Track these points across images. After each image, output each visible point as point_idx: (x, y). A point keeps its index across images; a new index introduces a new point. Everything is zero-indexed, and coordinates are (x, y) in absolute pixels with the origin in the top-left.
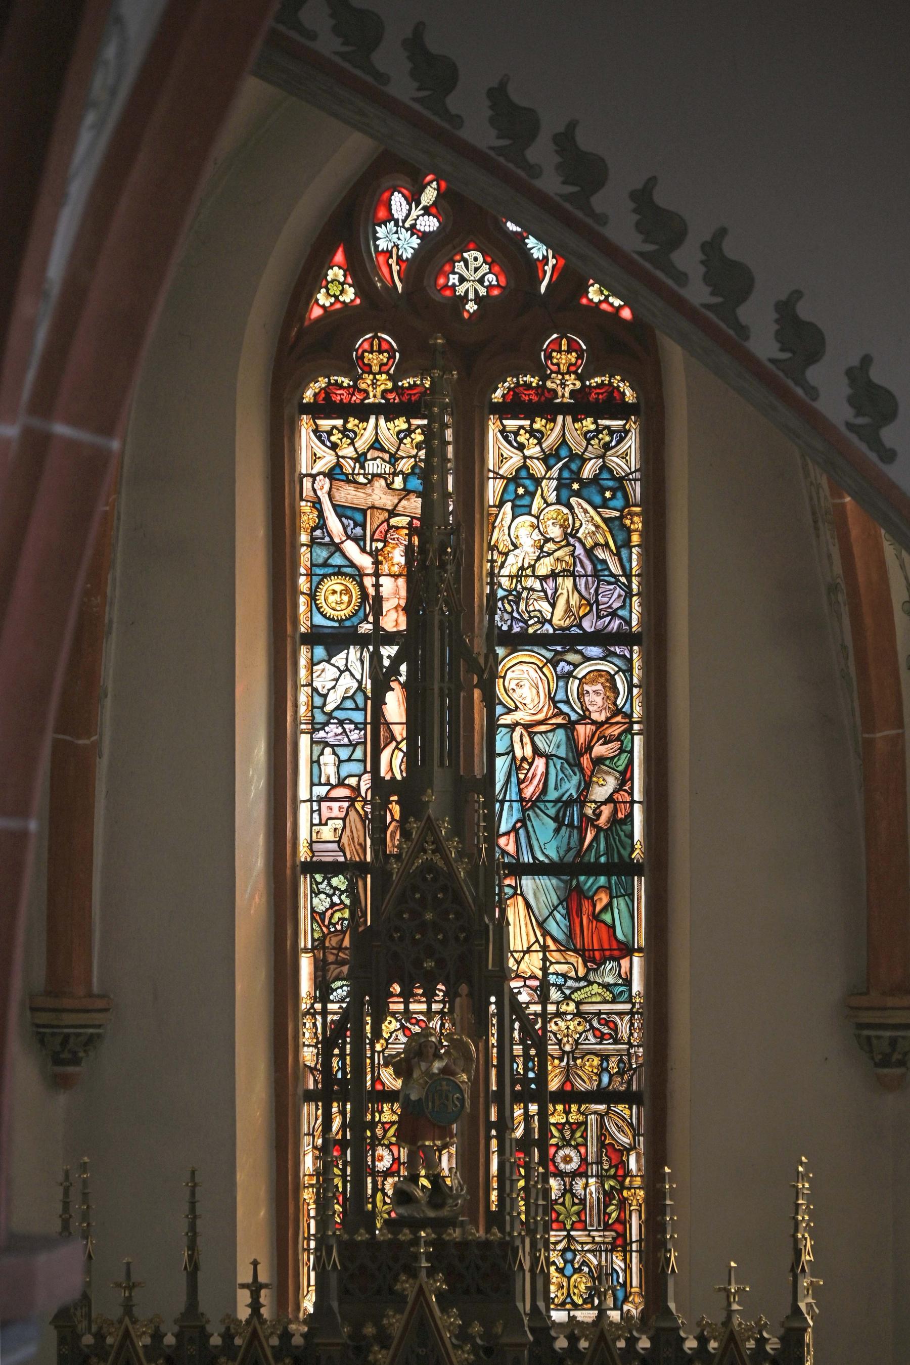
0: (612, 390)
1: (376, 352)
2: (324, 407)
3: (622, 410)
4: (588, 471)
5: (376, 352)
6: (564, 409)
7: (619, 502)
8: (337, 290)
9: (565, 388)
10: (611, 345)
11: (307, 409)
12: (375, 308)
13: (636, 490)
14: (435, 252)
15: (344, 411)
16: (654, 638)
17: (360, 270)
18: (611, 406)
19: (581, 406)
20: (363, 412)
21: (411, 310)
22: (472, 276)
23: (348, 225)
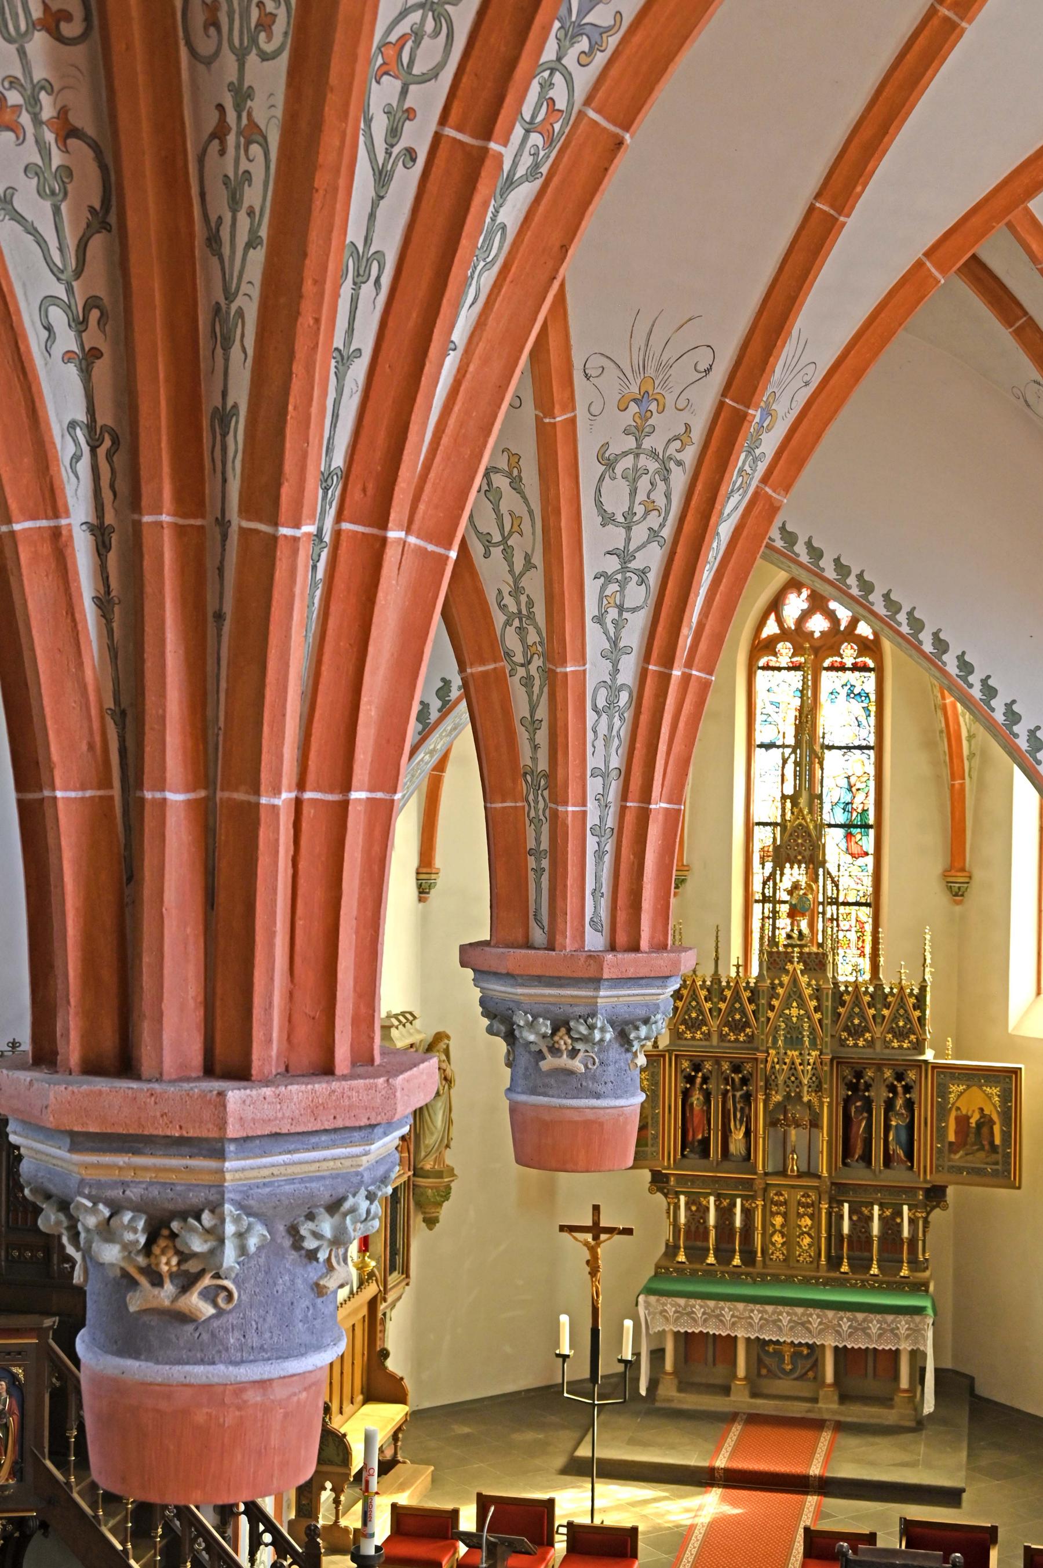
0: (865, 663)
1: (785, 648)
2: (767, 668)
3: (869, 670)
4: (856, 691)
5: (785, 648)
6: (849, 669)
7: (867, 701)
8: (771, 628)
9: (849, 662)
10: (867, 647)
11: (760, 668)
12: (785, 634)
13: (873, 697)
14: (805, 615)
15: (773, 669)
16: (878, 748)
17: (780, 621)
18: (865, 668)
19: (855, 668)
20: (779, 669)
21: (797, 636)
22: (818, 624)
23: (775, 605)
